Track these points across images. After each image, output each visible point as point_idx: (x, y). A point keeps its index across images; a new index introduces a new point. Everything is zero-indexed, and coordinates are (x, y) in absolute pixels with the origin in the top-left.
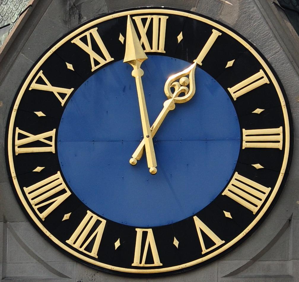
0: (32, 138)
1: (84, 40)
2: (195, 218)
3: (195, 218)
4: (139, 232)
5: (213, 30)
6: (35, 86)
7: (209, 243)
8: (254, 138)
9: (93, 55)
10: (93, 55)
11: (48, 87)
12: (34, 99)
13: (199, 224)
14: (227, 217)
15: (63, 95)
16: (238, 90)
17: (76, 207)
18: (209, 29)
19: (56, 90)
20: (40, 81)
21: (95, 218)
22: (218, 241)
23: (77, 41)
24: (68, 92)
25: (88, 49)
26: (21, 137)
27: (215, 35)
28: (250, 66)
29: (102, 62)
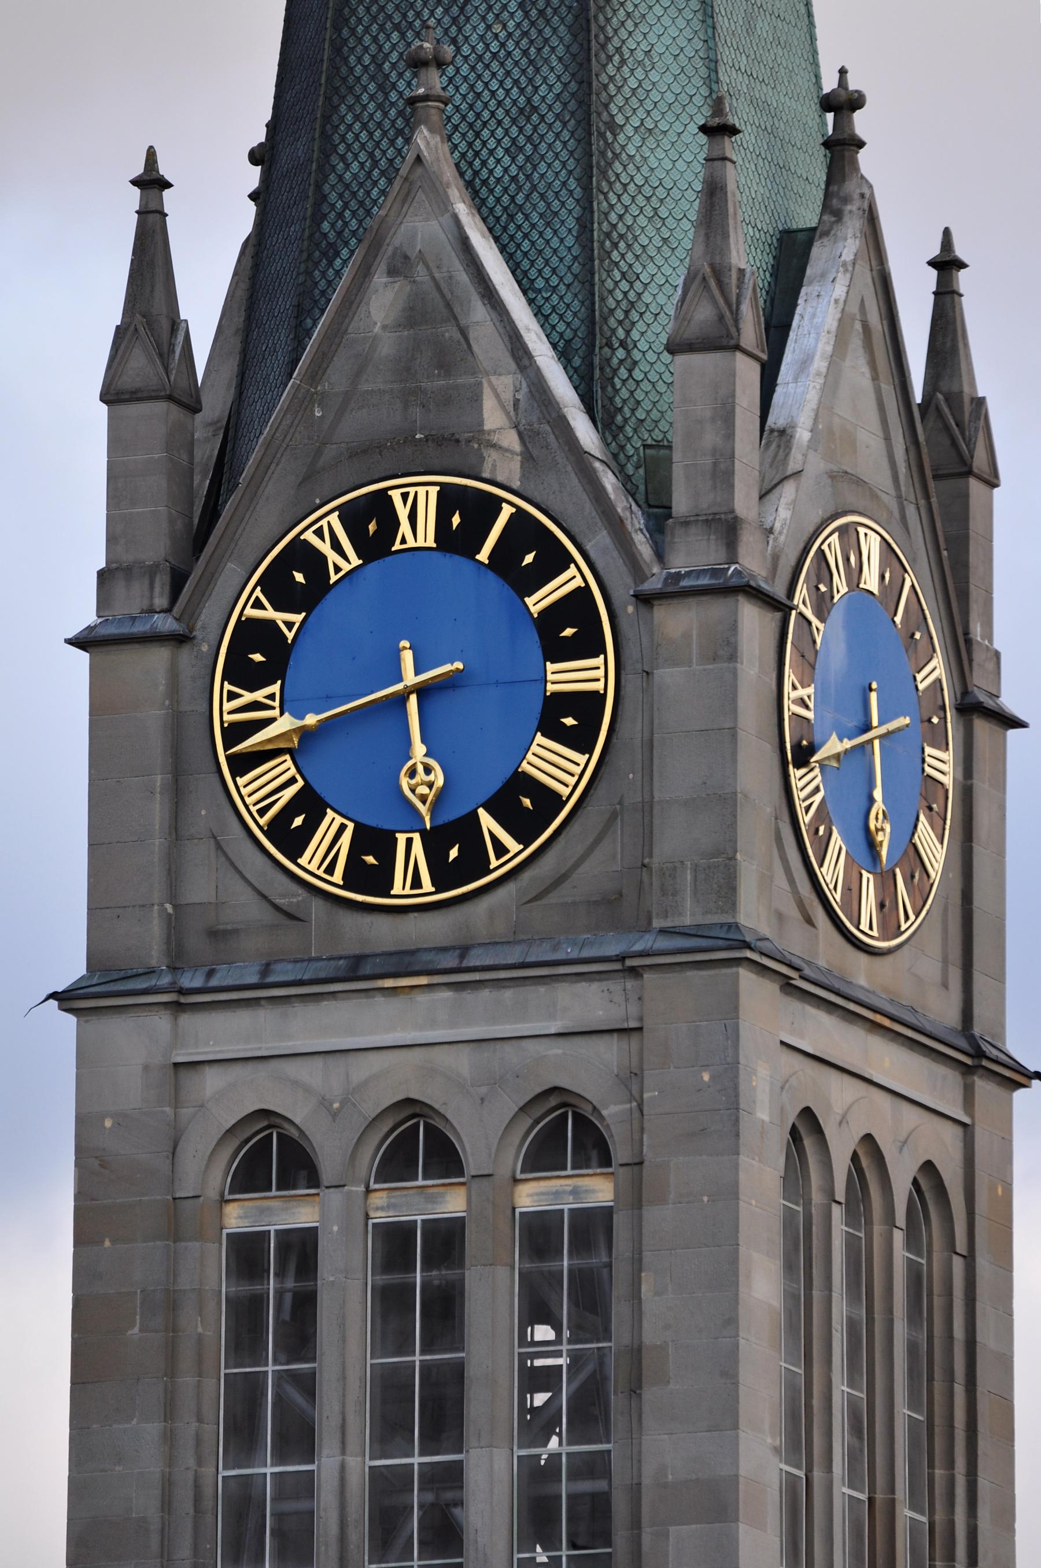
0: (248, 697)
1: (319, 532)
2: (481, 811)
3: (481, 811)
4: (401, 838)
5: (504, 505)
6: (250, 612)
7: (501, 850)
8: (565, 676)
9: (332, 557)
10: (332, 557)
11: (270, 613)
12: (254, 634)
13: (487, 821)
14: (525, 805)
15: (290, 625)
16: (537, 602)
17: (311, 804)
18: (497, 503)
19: (280, 617)
20: (258, 605)
21: (339, 820)
22: (512, 845)
23: (309, 536)
24: (297, 618)
25: (325, 547)
26: (232, 696)
27: (507, 511)
28: (555, 561)
29: (346, 567)
